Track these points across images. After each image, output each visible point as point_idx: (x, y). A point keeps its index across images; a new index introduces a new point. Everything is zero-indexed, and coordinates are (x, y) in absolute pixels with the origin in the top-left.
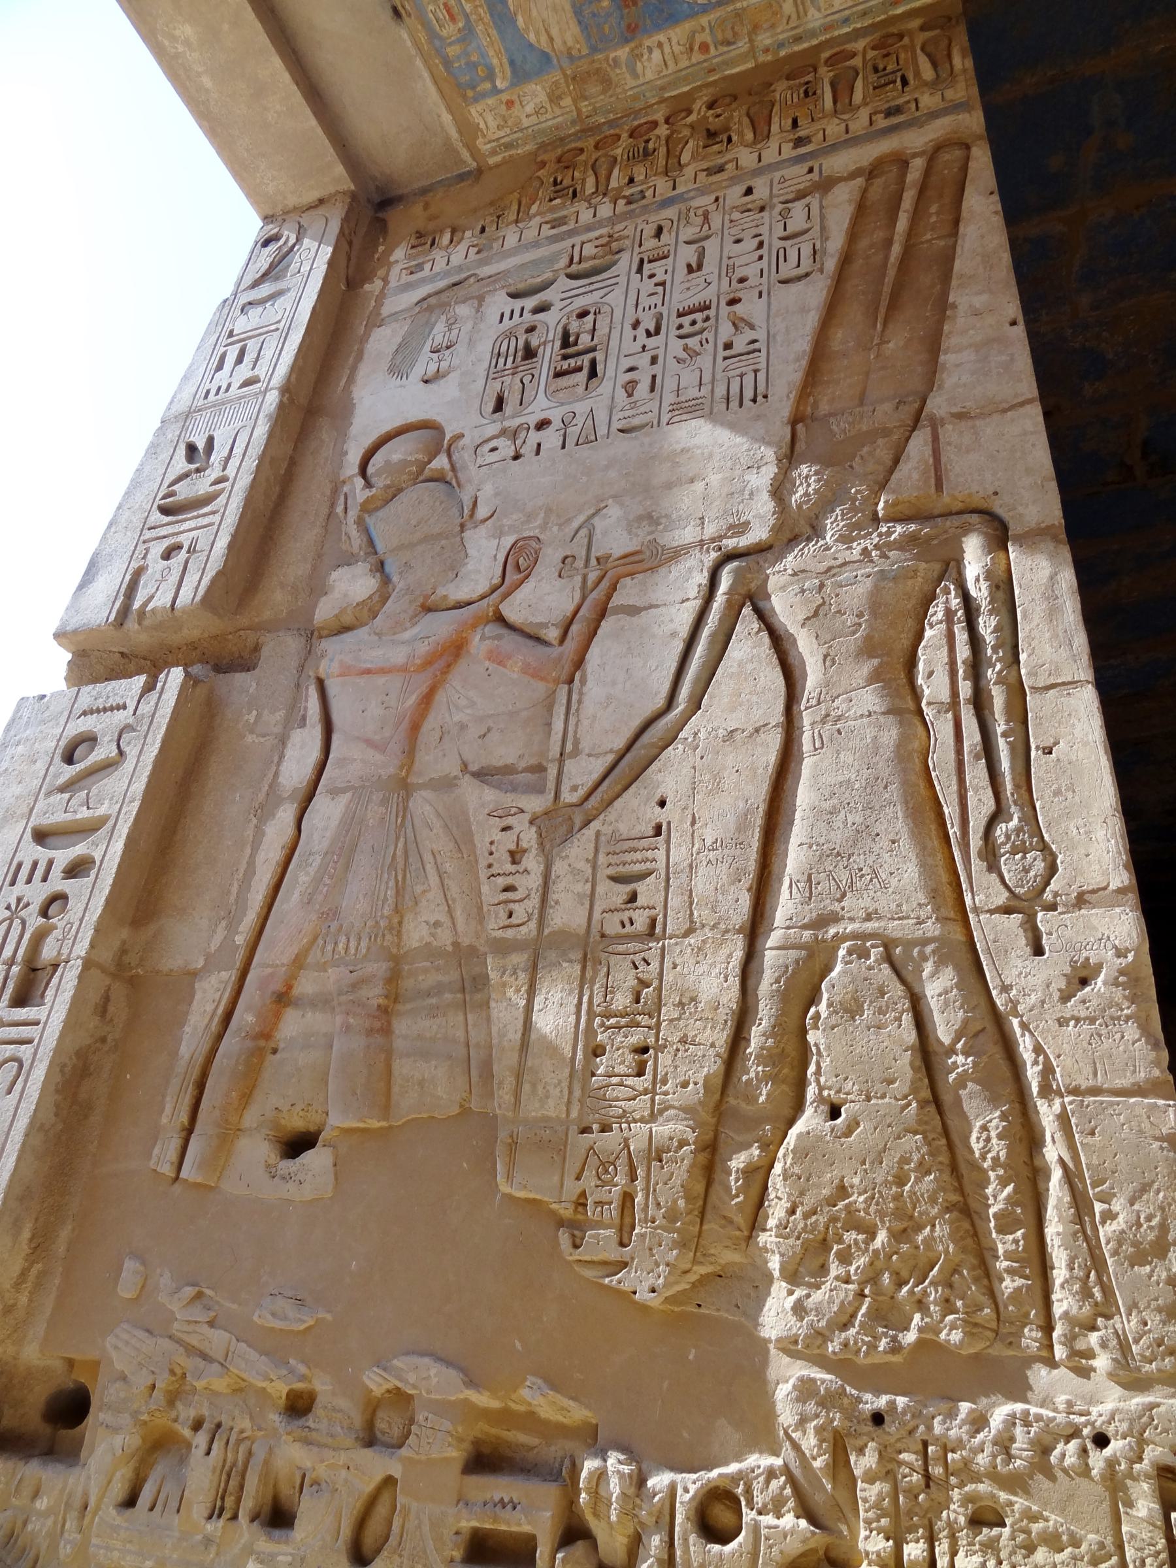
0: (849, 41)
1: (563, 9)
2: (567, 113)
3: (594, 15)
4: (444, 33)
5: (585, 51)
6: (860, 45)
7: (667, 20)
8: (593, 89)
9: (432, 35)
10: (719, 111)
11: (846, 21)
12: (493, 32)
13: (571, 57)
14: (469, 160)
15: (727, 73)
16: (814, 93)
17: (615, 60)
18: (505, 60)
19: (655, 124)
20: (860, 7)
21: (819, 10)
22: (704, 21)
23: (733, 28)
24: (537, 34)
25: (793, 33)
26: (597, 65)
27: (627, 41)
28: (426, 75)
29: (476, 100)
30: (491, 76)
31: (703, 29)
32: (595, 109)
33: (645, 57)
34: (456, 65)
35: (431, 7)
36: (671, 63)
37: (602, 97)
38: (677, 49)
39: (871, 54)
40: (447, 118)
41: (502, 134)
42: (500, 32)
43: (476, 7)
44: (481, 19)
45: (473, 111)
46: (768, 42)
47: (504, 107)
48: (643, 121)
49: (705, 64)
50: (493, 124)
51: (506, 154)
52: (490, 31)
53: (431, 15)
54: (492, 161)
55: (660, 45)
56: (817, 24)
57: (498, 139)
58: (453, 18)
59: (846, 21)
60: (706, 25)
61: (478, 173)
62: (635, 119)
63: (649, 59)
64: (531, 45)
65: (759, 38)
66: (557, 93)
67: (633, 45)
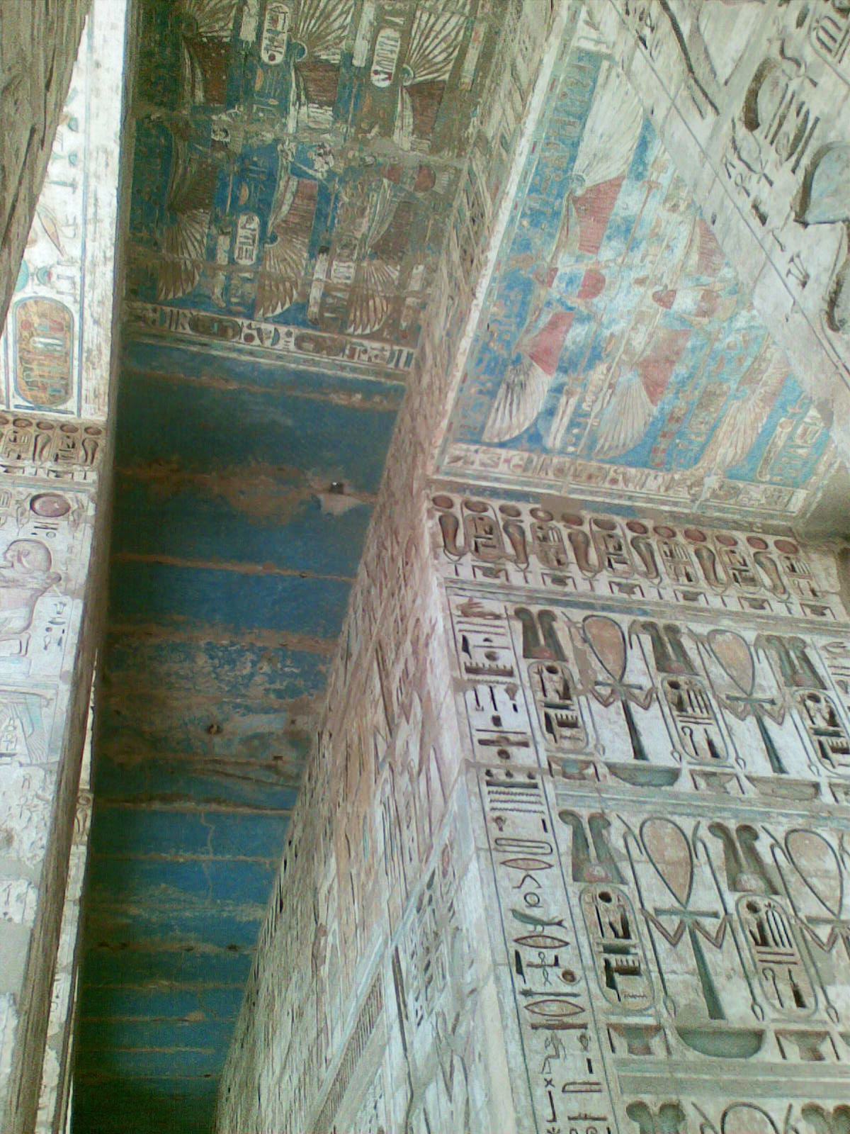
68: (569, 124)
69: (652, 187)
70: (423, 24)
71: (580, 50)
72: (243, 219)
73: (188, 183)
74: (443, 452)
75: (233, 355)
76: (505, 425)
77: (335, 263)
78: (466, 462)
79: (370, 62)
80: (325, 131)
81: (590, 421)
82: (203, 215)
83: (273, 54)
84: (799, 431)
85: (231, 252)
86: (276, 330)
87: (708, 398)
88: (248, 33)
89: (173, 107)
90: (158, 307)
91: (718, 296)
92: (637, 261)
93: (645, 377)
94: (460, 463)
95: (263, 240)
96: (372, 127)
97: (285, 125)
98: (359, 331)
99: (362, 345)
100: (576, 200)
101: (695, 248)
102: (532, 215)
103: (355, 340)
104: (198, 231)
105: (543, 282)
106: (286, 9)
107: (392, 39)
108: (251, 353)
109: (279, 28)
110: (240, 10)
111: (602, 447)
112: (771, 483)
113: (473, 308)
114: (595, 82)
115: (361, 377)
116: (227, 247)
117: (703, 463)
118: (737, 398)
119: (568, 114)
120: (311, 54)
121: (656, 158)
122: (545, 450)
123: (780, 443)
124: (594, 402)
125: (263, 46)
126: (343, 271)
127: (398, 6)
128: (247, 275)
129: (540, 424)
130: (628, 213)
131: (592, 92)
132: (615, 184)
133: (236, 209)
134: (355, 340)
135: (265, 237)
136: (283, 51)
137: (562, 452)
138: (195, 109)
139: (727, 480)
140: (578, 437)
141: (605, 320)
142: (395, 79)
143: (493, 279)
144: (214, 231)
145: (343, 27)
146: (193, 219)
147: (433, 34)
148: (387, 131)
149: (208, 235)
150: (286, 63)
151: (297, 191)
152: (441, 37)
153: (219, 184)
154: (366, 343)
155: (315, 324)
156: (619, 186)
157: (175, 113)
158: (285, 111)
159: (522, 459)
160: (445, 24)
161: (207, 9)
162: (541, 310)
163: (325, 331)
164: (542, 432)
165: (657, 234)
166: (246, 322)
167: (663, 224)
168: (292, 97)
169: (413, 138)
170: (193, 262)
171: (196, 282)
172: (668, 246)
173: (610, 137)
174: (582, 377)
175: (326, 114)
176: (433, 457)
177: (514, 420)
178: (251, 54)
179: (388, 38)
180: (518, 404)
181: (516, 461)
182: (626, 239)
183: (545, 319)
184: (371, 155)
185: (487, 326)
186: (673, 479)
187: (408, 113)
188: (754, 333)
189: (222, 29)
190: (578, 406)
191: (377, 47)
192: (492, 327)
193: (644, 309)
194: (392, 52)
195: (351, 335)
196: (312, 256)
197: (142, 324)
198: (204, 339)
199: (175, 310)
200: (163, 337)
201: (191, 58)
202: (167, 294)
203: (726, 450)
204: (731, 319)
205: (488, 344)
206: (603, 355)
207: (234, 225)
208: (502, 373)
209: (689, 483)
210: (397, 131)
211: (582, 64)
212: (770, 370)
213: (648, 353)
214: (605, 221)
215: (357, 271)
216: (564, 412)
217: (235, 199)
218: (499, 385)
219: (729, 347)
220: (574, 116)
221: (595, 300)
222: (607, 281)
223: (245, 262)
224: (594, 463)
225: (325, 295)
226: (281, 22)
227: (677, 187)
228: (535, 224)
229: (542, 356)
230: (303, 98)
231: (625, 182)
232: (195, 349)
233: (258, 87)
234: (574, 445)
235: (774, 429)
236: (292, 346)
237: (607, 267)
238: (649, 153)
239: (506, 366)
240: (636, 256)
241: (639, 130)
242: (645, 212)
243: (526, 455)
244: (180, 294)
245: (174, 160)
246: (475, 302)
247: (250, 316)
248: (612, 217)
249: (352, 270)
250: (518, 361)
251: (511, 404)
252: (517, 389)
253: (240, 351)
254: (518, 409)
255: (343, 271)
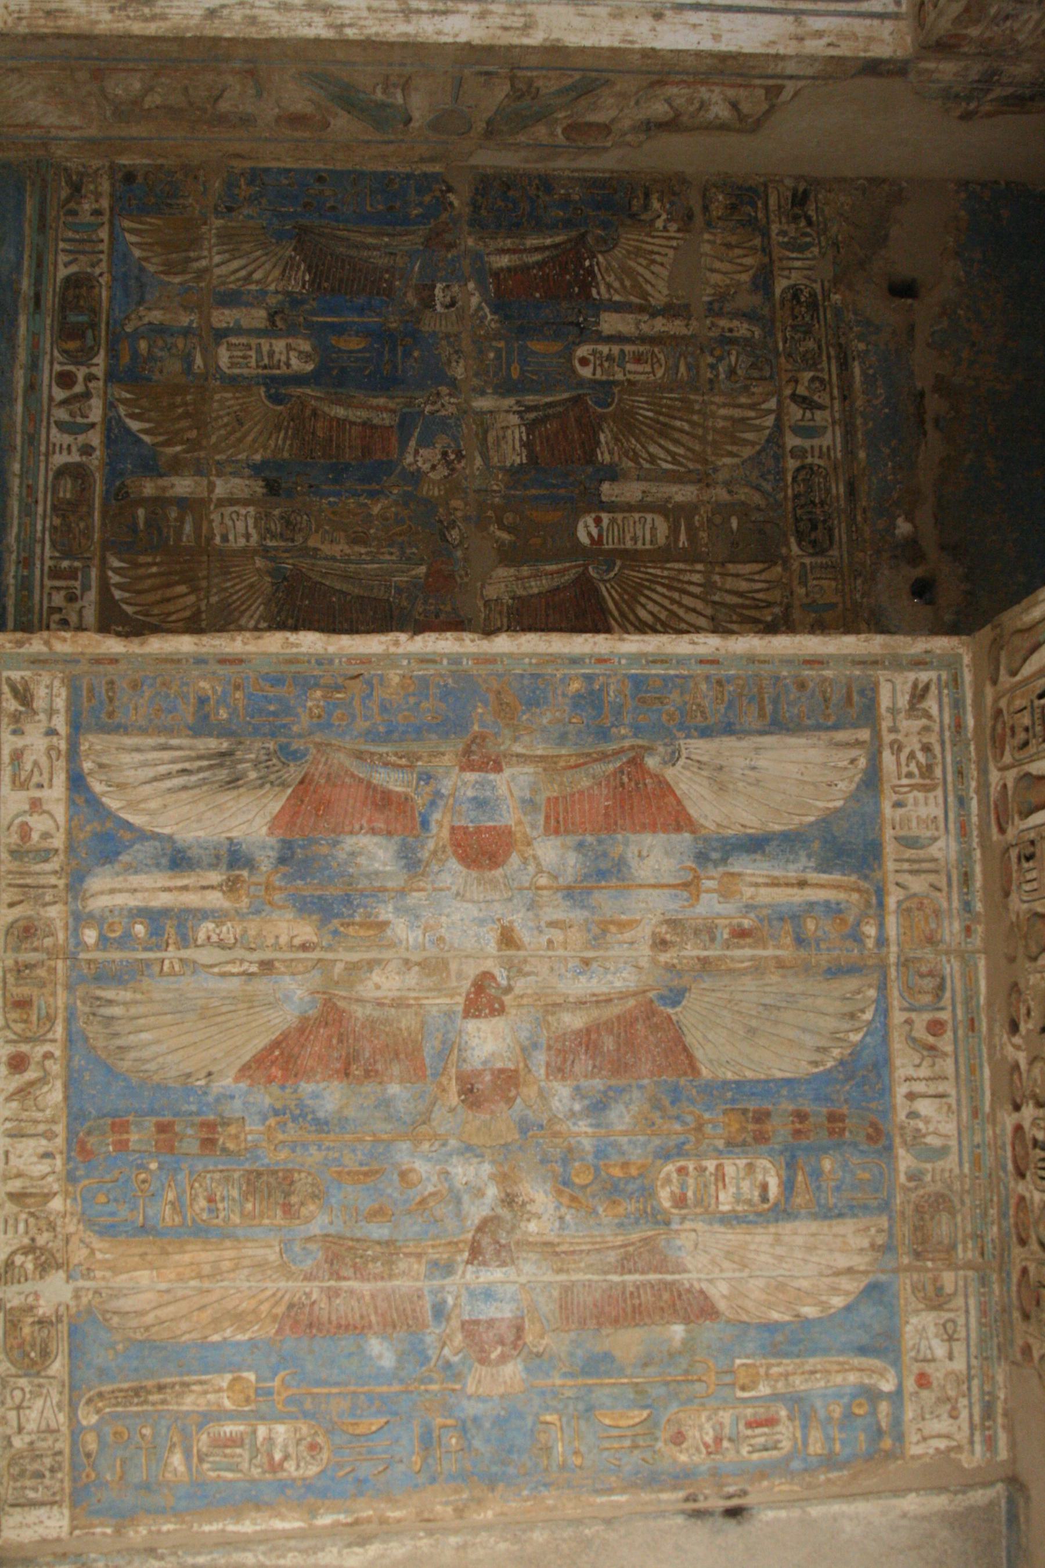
0: (988, 795)
1: (813, 1235)
2: (966, 1286)
3: (838, 1188)
4: (786, 1445)
5: (884, 1222)
6: (994, 776)
7: (879, 1076)
8: (942, 1228)
9: (780, 1468)
10: (1023, 1010)
11: (962, 802)
12: (812, 1362)
13: (887, 1248)
14: (990, 1493)
15: (982, 1000)
16: (1032, 843)
17: (911, 1178)
18: (856, 1361)
19: (1019, 1128)
20: (950, 778)
21: (935, 839)
22: (898, 1017)
23: (922, 976)
24: (835, 1290)
25: (955, 883)
26: (909, 1211)
27: (889, 1148)
28: (836, 1508)
29: (900, 1438)
30: (873, 1395)
31: (909, 1022)
32: (978, 1237)
33: (921, 1125)
34: (838, 1447)
35: (745, 1450)
36: (941, 1087)
37: (959, 1218)
38: (924, 1072)
39: (1007, 759)
40: (911, 1503)
41: (964, 1414)
42: (813, 1353)
43: (767, 1374)
44: (786, 1375)
45: (915, 1450)
46: (957, 926)
47: (925, 1393)
48: (1009, 1154)
49: (960, 1032)
50: (942, 1425)
51: (1000, 1420)
52: (807, 1368)
53: (755, 1456)
54: (1003, 1454)
55: (911, 1096)
56: (953, 846)
57: (972, 1427)
58: (771, 1422)
59: (962, 802)
60: (906, 1015)
61: (1015, 1483)
62: (1005, 1171)
63: (927, 1121)
64: (848, 1308)
65: (947, 938)
66: (930, 1289)
67: (898, 1140)
68: (762, 709)
69: (691, 886)
70: (686, 577)
71: (875, 688)
72: (306, 346)
73: (353, 253)
74: (37, 661)
75: (22, 356)
76: (131, 775)
77: (251, 509)
78: (16, 717)
79: (611, 508)
80: (485, 458)
81: (172, 952)
82: (298, 282)
83: (588, 362)
84: (230, 1429)
85: (238, 330)
86: (93, 425)
87: (274, 1188)
88: (611, 323)
89: (477, 223)
90: (106, 218)
91: (510, 1101)
92: (550, 913)
93: (301, 1030)
94: (12, 705)
95: (271, 381)
96: (508, 529)
97: (483, 393)
98: (115, 579)
99: (85, 588)
100: (636, 762)
101: (595, 1013)
102: (591, 693)
103: (94, 573)
104: (270, 273)
105: (468, 752)
106: (660, 373)
107: (653, 536)
108: (32, 387)
109: (630, 367)
110: (641, 309)
111: (110, 1002)
112: (76, 1431)
113: (391, 636)
114: (836, 727)
115: (10, 603)
116: (245, 323)
117: (103, 1249)
118: (286, 1246)
119: (775, 702)
120: (602, 417)
121: (740, 875)
122: (76, 883)
123: (189, 1403)
124: (221, 945)
125: (600, 348)
126: (238, 528)
127: (703, 535)
128: (199, 361)
129: (143, 851)
130: (634, 863)
131: (818, 727)
132: (680, 820)
133: (318, 332)
134: (94, 573)
135: (277, 385)
136: (598, 376)
137: (79, 919)
138: (478, 256)
139: (63, 1328)
140: (126, 940)
141: (414, 898)
142: (595, 552)
143: (455, 659)
144: (272, 301)
145: (652, 459)
146: (289, 266)
147: (676, 595)
148: (509, 556)
149: (264, 293)
150: (581, 382)
151: (374, 427)
152: (675, 608)
153: (361, 300)
154: (92, 595)
155: (119, 497)
156: (678, 829)
157: (466, 228)
158: (506, 388)
159: (46, 836)
160: (694, 610)
161: (631, 263)
162: (411, 767)
163: (104, 514)
164: (124, 858)
165: (605, 931)
166: (99, 371)
167: (628, 936)
168: (530, 399)
169: (507, 599)
170: (206, 270)
171: (166, 278)
172: (586, 962)
173: (757, 783)
174: (277, 897)
175: (516, 457)
176: (20, 644)
177: (148, 789)
178: (582, 330)
179: (653, 528)
180: (185, 788)
181: (39, 824)
182: (586, 877)
183: (394, 782)
184: (463, 539)
185: (360, 674)
186: (48, 1196)
187: (546, 584)
188: (441, 1210)
189: (609, 286)
190: (204, 914)
191: (637, 516)
192: (357, 686)
193: (453, 966)
194: (635, 539)
195: (103, 561)
196: (257, 470)
197: (64, 194)
198: (50, 300)
199: (104, 246)
200: (42, 227)
201: (556, 246)
202: (132, 231)
203: (146, 1289)
204: (468, 1150)
205: (317, 685)
206: (336, 922)
207: (292, 331)
208: (256, 731)
209: (41, 1241)
210: (512, 571)
211: (856, 697)
212: (366, 1288)
213: (360, 1012)
214: (609, 824)
215: (244, 551)
216: (185, 888)
217: (339, 330)
218: (224, 731)
219: (403, 1175)
220: (775, 711)
221: (454, 864)
222: (498, 873)
223: (224, 357)
224: (62, 998)
225: (182, 503)
226: (640, 368)
227: (697, 932)
228: (578, 701)
229: (311, 803)
230: (532, 416)
231: (687, 835)
232: (26, 285)
233: (536, 346)
234: (103, 942)
235: (220, 1370)
236: (59, 459)
237: (525, 861)
238: (745, 858)
239: (273, 735)
240: (556, 910)
241: (777, 828)
242: (643, 893)
243: (58, 841)
244: (137, 253)
245: (389, 229)
246: (403, 637)
247: (111, 376)
248: (619, 836)
249: (242, 542)
250: (289, 755)
251: (184, 771)
252: (223, 774)
253: (34, 366)
254: (170, 790)
255: (238, 528)
